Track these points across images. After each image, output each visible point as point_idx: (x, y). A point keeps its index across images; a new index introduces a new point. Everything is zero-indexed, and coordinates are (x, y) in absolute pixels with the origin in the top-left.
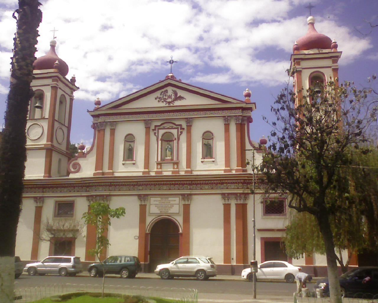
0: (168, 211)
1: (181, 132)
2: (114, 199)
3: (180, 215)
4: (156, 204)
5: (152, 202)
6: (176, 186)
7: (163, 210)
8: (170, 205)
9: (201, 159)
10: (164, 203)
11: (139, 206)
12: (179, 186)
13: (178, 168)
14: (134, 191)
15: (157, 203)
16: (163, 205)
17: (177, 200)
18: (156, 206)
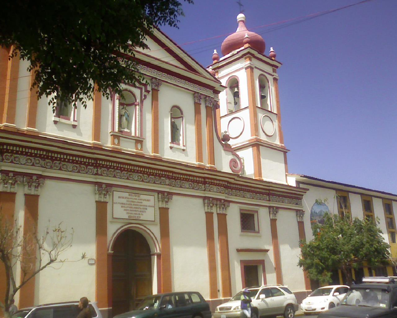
0: (140, 217)
1: (145, 96)
2: (48, 182)
3: (156, 225)
4: (122, 204)
5: (116, 199)
6: (150, 176)
7: (132, 214)
8: (142, 207)
9: (170, 143)
10: (135, 202)
11: (94, 205)
12: (155, 177)
13: (141, 150)
14: (86, 175)
15: (124, 201)
16: (133, 206)
17: (152, 198)
18: (122, 207)
